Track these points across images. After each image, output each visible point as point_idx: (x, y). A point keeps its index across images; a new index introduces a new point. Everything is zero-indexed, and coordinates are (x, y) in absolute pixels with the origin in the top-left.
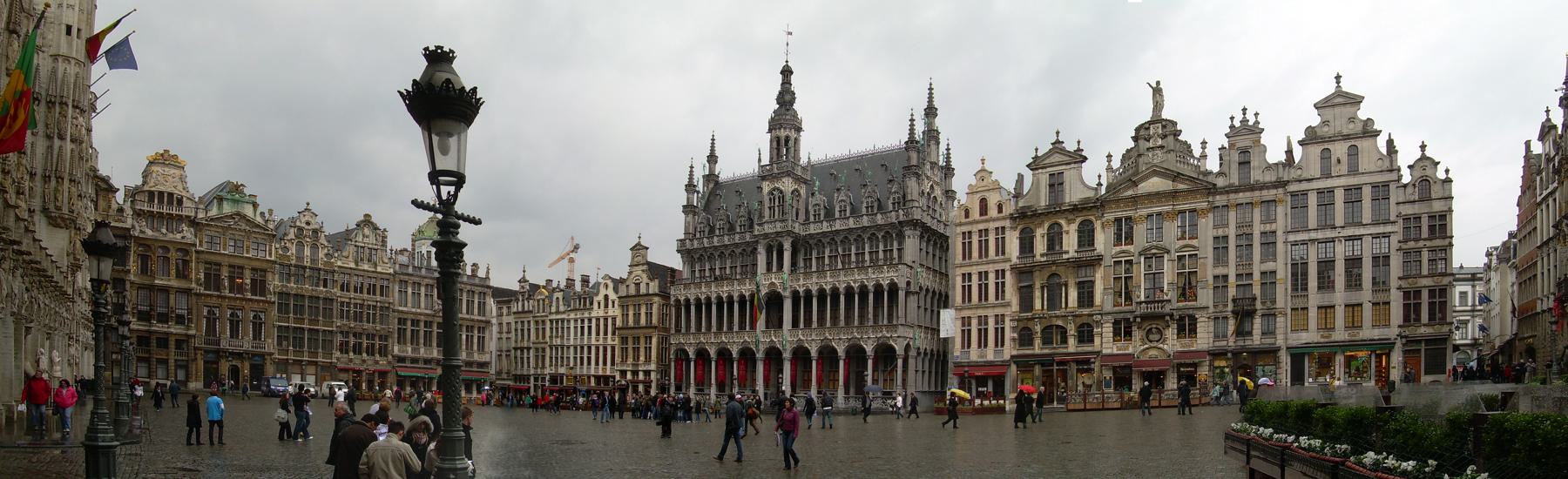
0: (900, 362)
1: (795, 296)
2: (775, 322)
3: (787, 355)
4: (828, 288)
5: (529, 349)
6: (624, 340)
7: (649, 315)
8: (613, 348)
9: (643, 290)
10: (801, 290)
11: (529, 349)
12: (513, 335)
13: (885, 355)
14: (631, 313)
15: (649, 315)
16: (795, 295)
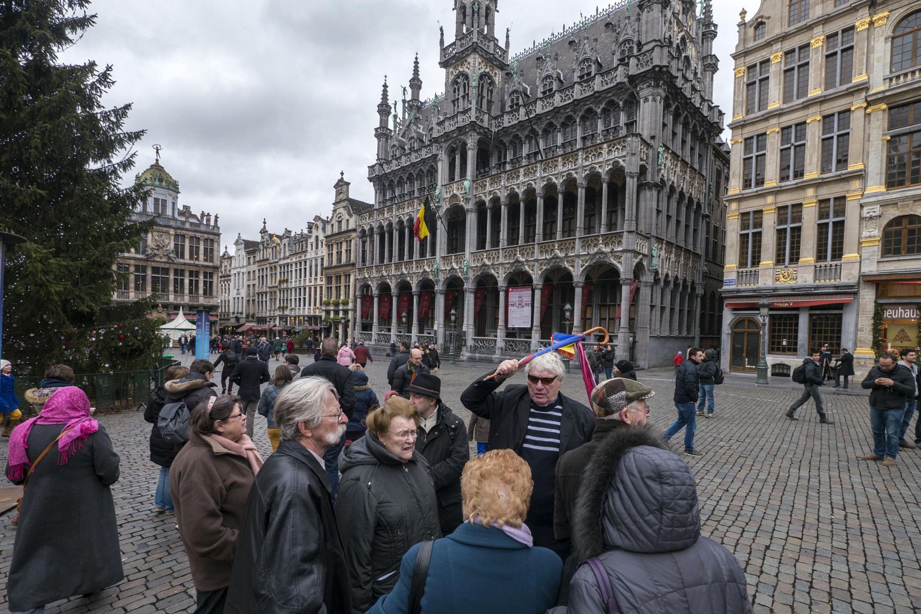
0: (625, 291)
1: (481, 207)
2: (455, 245)
3: (469, 285)
4: (520, 191)
5: (266, 293)
6: (329, 280)
7: (348, 251)
8: (321, 287)
9: (344, 228)
10: (487, 199)
11: (266, 293)
12: (256, 282)
13: (604, 282)
14: (335, 252)
15: (348, 251)
16: (481, 205)
